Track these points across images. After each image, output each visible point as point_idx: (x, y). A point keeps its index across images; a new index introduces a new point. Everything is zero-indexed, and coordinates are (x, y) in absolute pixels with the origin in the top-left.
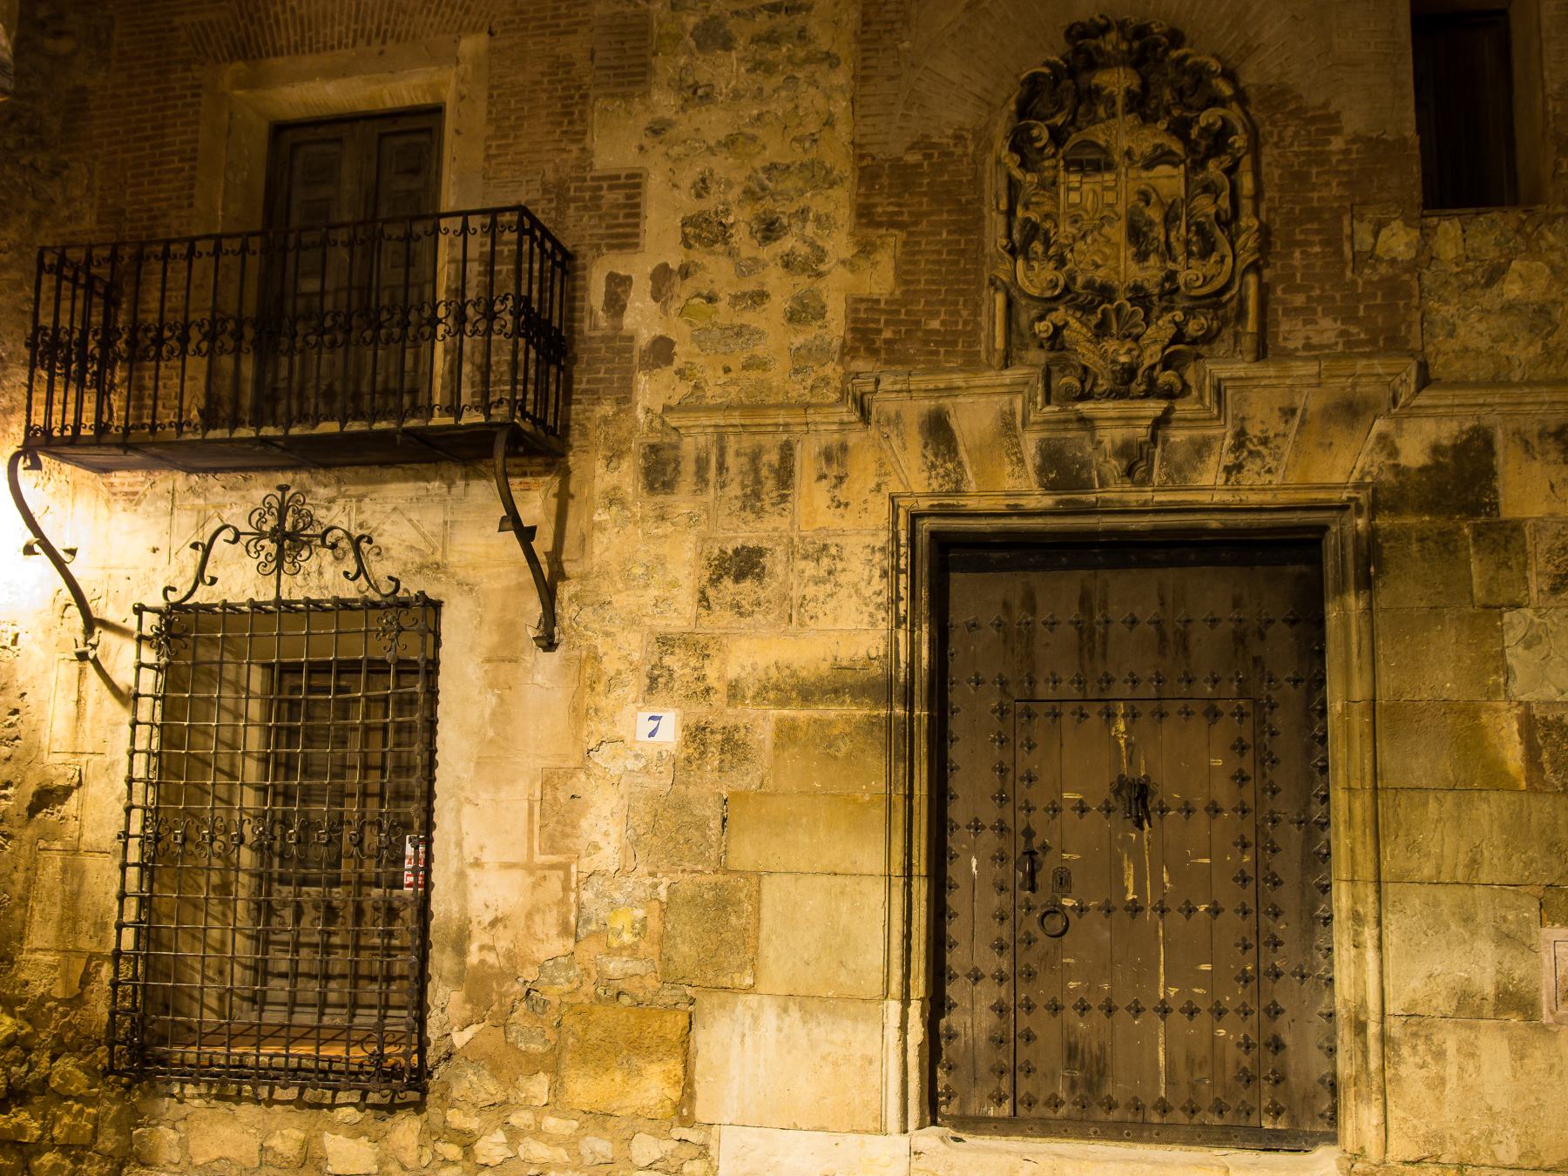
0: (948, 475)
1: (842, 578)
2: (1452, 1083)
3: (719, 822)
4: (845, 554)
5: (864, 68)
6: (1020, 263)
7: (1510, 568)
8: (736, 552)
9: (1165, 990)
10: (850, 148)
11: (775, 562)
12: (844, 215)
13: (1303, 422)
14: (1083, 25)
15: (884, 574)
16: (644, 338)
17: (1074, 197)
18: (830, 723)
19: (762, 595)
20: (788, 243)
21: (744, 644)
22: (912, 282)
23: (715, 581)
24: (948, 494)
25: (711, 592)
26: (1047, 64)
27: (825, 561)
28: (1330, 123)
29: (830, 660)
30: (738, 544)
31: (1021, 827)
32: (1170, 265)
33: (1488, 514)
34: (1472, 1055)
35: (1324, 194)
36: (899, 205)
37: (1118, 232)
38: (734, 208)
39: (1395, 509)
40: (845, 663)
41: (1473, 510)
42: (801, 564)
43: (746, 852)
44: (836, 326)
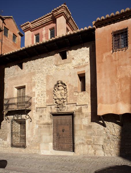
9: (66, 142)
12: (46, 94)
16: (35, 102)
28: (73, 86)
37: (60, 95)
39: (76, 112)
41: (81, 112)
44: (46, 102)
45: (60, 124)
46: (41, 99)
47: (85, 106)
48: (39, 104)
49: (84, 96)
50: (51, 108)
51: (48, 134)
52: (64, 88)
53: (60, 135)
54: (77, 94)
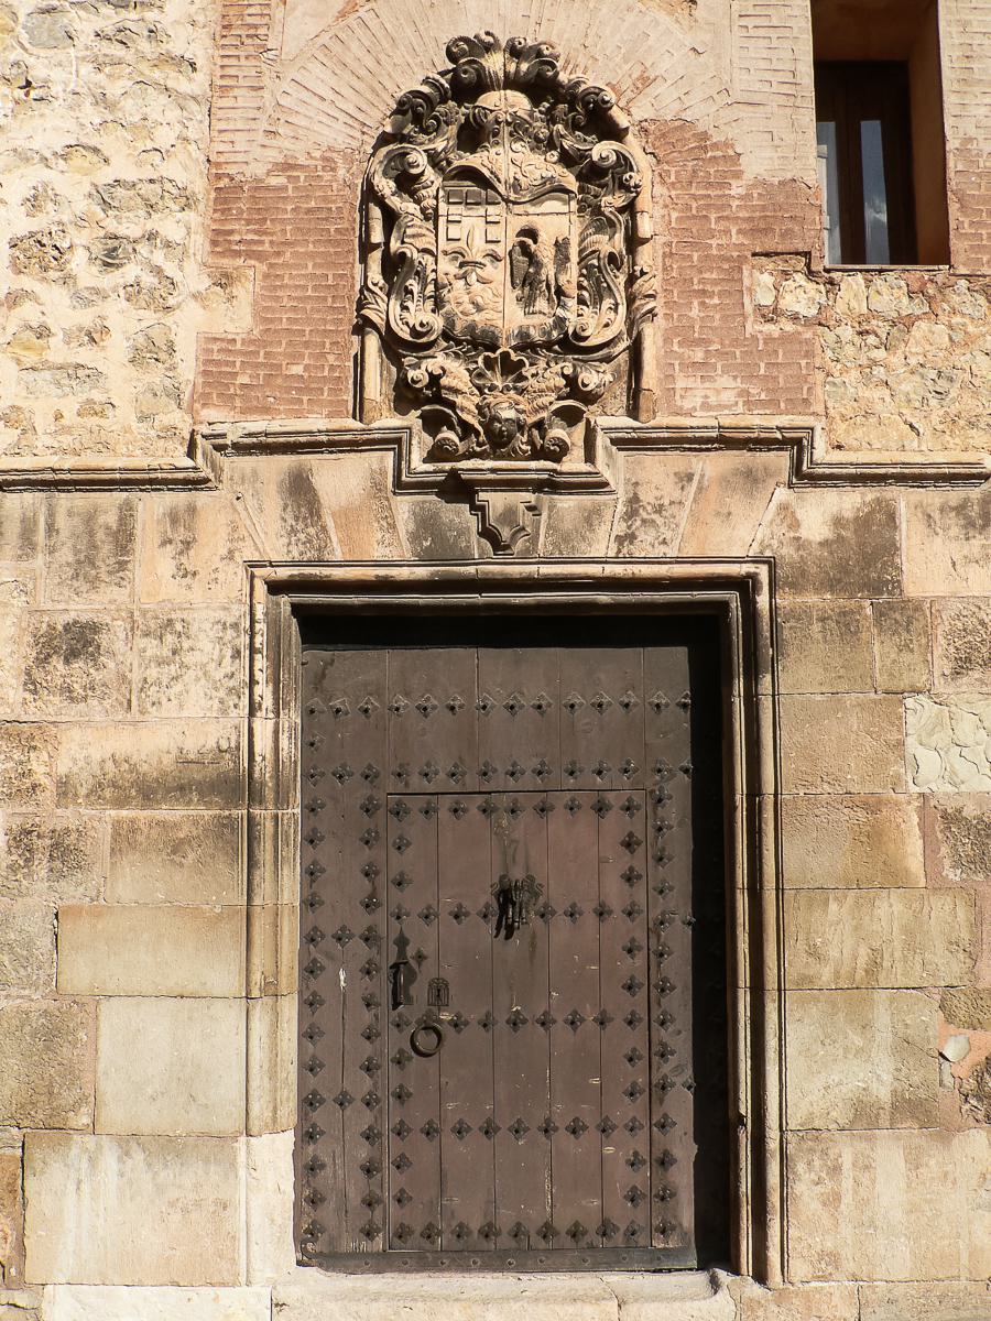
0: (310, 541)
1: (188, 659)
2: (847, 1199)
3: (48, 941)
4: (193, 629)
5: (222, 77)
6: (395, 306)
7: (912, 651)
8: (67, 628)
10: (204, 167)
11: (114, 639)
12: (199, 243)
13: (700, 489)
14: (466, 40)
15: (237, 654)
17: (454, 231)
18: (176, 826)
19: (97, 676)
20: (131, 272)
21: (76, 733)
22: (271, 321)
23: (43, 660)
24: (309, 563)
25: (38, 675)
26: (426, 81)
27: (170, 639)
29: (175, 752)
30: (70, 617)
31: (394, 936)
32: (560, 312)
33: (889, 593)
34: (867, 1167)
35: (723, 241)
36: (256, 232)
37: (498, 273)
38: (71, 229)
39: (796, 586)
40: (192, 756)
41: (875, 588)
42: (141, 642)
43: (79, 973)
44: (188, 370)
45: (440, 781)
46: (86, 318)
47: (954, 495)
48: (43, 422)
49: (929, 336)
50: (300, 490)
51: (224, 976)
52: (592, 174)
53: (439, 992)
54: (801, 296)
